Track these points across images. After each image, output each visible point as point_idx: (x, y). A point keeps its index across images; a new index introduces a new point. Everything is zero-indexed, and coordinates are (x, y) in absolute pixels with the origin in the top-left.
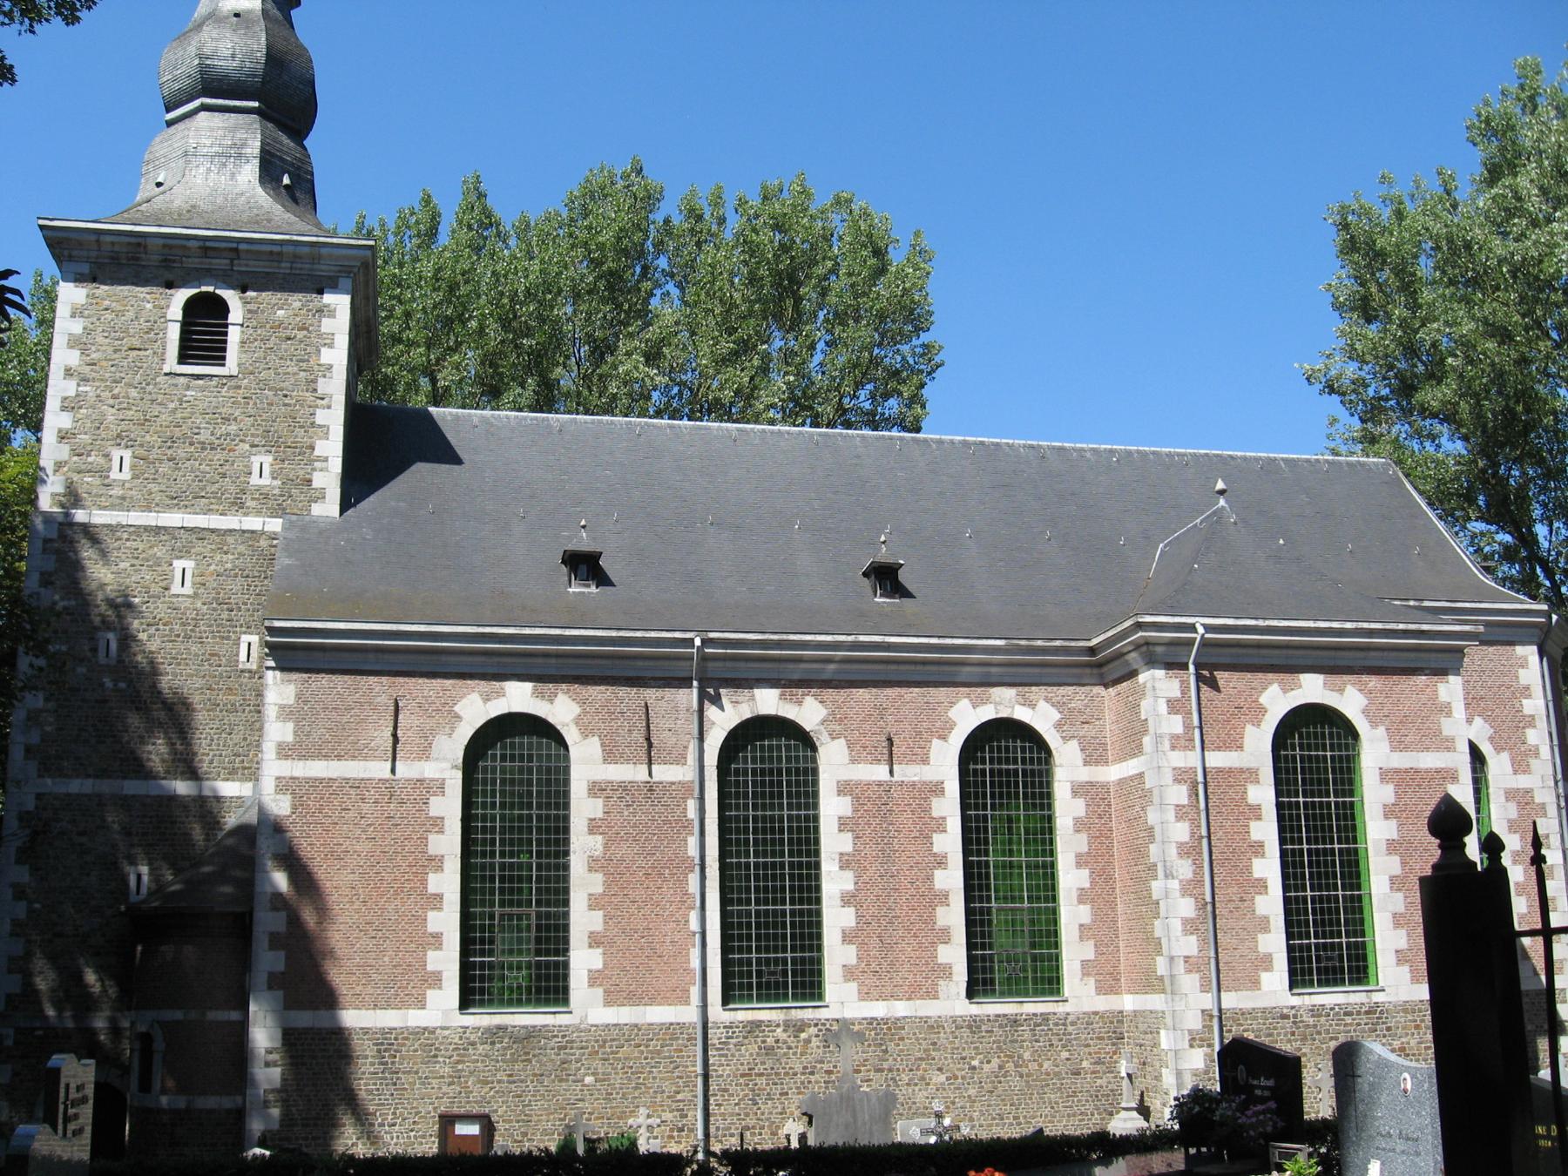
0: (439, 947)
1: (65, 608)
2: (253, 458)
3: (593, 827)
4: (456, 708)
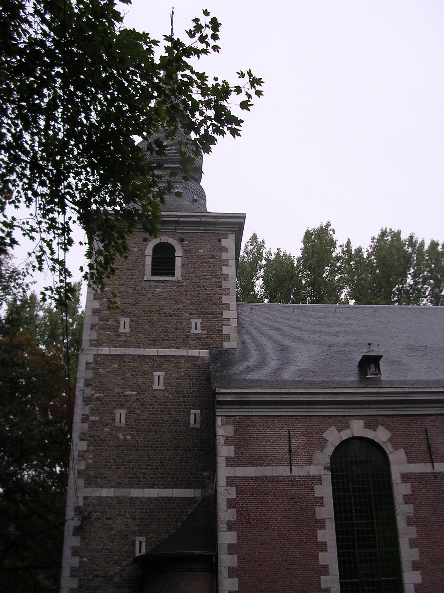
0: (327, 573)
1: (98, 397)
2: (192, 320)
3: (407, 499)
4: (324, 435)
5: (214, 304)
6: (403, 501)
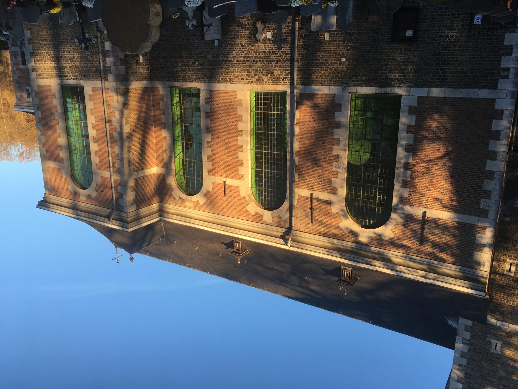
5: (475, 360)
6: (339, 174)
